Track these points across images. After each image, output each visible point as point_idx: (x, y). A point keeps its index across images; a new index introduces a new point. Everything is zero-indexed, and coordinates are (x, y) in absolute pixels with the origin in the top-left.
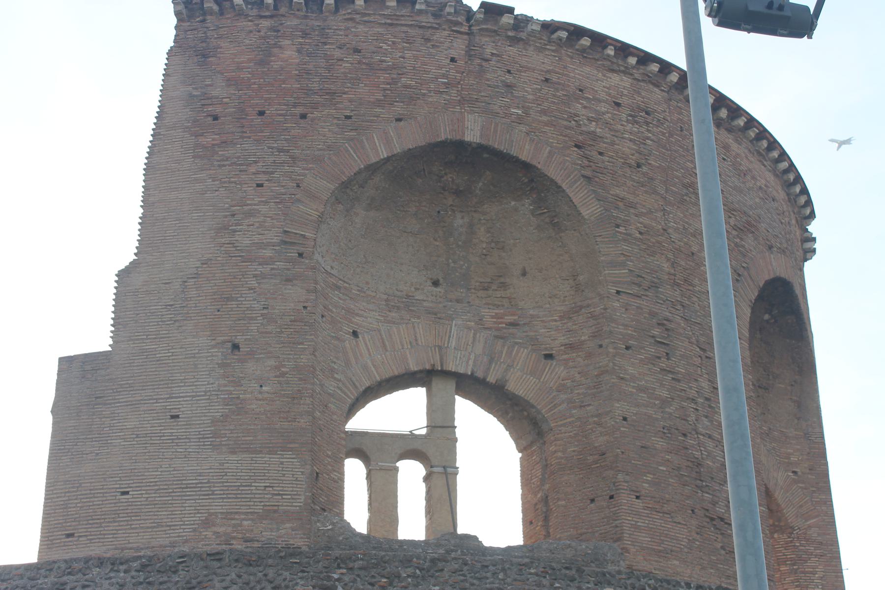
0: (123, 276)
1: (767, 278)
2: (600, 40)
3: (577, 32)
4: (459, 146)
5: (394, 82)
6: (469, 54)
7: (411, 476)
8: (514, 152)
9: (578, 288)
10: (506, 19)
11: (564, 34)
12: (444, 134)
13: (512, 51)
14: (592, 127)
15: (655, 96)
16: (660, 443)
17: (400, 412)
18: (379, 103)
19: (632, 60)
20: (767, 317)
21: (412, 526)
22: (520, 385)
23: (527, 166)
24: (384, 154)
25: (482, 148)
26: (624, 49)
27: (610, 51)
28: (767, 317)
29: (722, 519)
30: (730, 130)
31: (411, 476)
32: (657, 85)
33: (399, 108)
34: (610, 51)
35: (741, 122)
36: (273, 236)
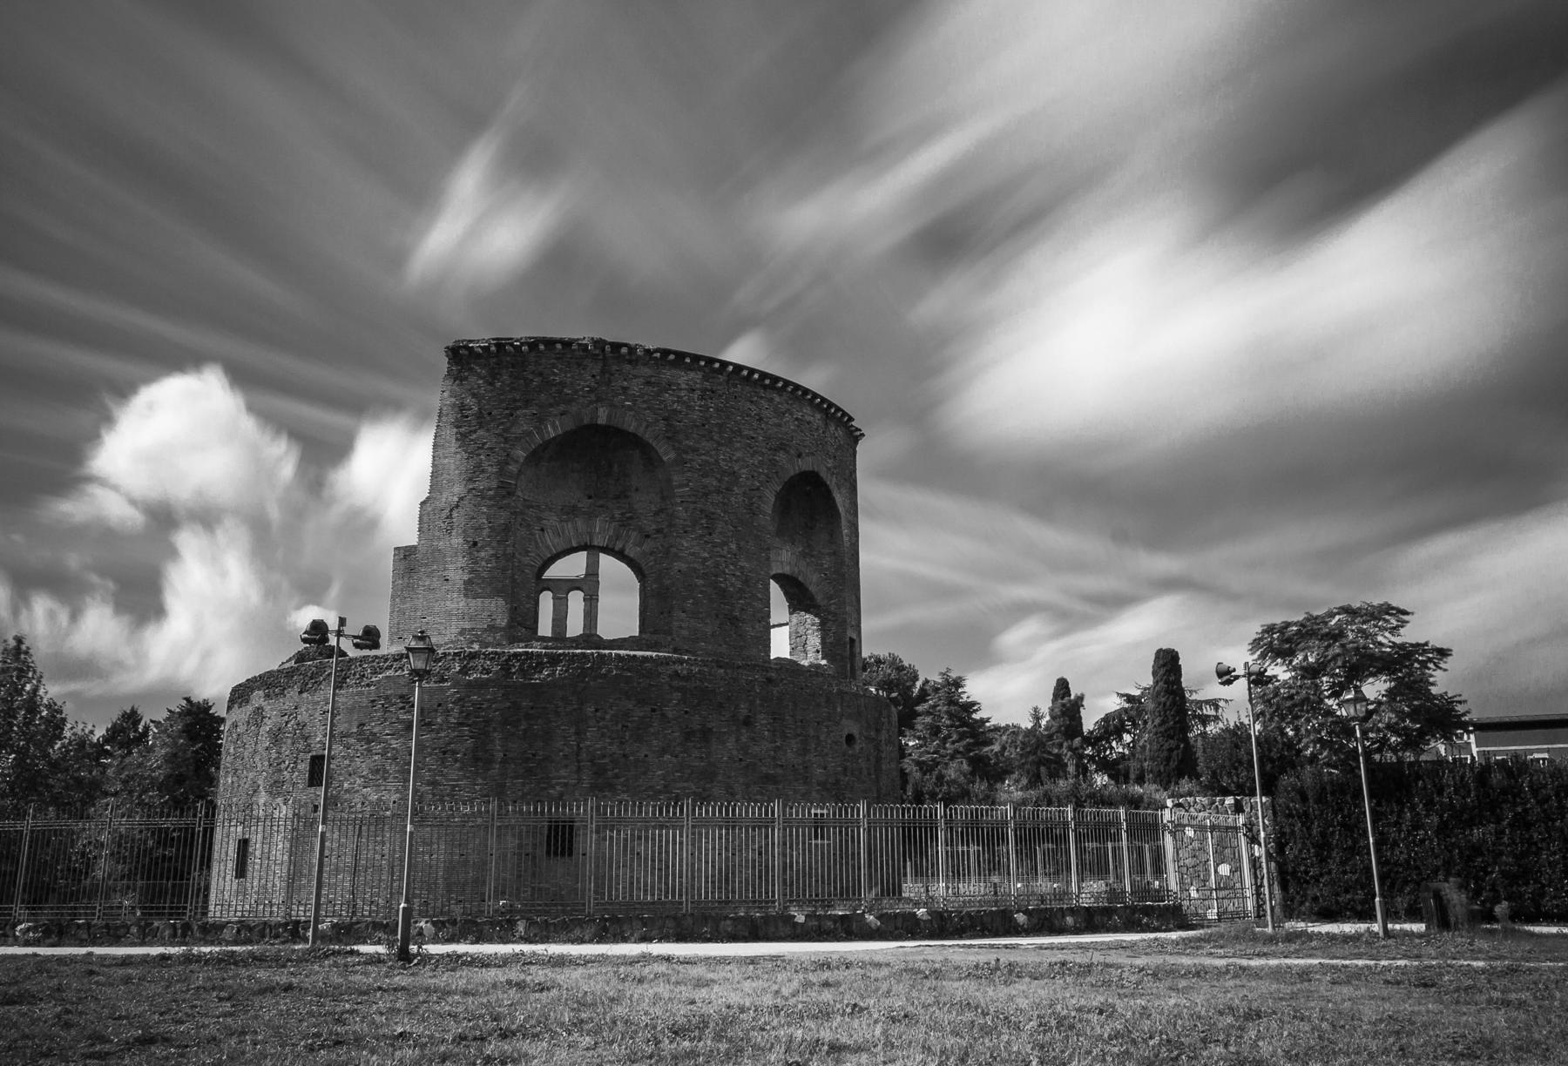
0: (423, 504)
2: (681, 356)
4: (594, 428)
5: (560, 392)
6: (603, 372)
7: (576, 601)
8: (625, 427)
9: (663, 498)
10: (624, 350)
13: (628, 367)
17: (572, 566)
18: (551, 405)
21: (575, 627)
22: (631, 552)
23: (635, 435)
24: (553, 435)
29: (736, 618)
31: (576, 601)
33: (562, 407)
36: (494, 484)
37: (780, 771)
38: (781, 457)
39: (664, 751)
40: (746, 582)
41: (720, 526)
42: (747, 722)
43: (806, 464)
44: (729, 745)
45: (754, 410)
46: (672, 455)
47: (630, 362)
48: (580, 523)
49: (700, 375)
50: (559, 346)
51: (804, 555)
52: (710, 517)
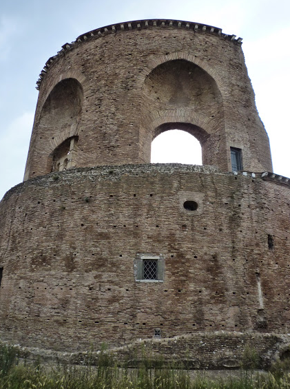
1: (160, 63)
2: (88, 34)
3: (81, 37)
4: (59, 83)
10: (68, 46)
11: (79, 40)
12: (56, 83)
14: (89, 57)
15: (111, 38)
16: (91, 133)
19: (99, 33)
20: (190, 73)
25: (63, 81)
26: (95, 32)
27: (92, 35)
28: (190, 73)
30: (146, 28)
32: (111, 33)
34: (92, 35)
35: (147, 24)
37: (112, 230)
38: (152, 56)
39: (40, 225)
40: (121, 125)
41: (104, 103)
42: (87, 201)
43: (171, 57)
44: (76, 216)
45: (132, 41)
46: (84, 78)
47: (72, 50)
48: (67, 131)
49: (101, 39)
50: (51, 61)
51: (196, 111)
52: (100, 100)
